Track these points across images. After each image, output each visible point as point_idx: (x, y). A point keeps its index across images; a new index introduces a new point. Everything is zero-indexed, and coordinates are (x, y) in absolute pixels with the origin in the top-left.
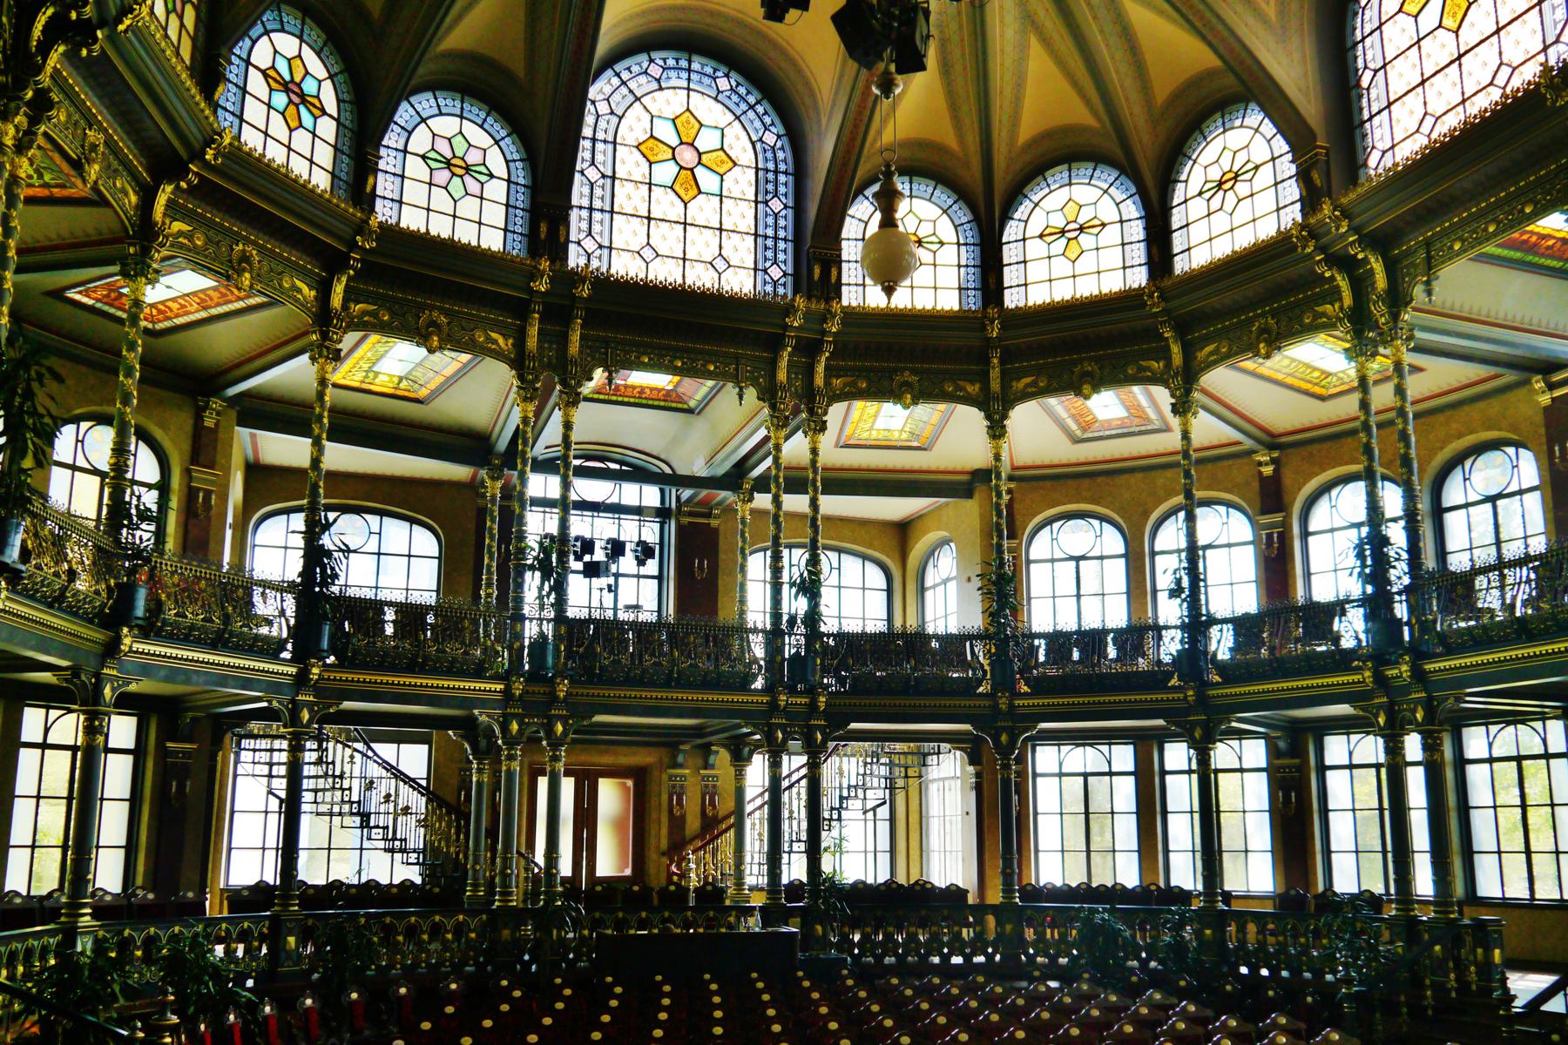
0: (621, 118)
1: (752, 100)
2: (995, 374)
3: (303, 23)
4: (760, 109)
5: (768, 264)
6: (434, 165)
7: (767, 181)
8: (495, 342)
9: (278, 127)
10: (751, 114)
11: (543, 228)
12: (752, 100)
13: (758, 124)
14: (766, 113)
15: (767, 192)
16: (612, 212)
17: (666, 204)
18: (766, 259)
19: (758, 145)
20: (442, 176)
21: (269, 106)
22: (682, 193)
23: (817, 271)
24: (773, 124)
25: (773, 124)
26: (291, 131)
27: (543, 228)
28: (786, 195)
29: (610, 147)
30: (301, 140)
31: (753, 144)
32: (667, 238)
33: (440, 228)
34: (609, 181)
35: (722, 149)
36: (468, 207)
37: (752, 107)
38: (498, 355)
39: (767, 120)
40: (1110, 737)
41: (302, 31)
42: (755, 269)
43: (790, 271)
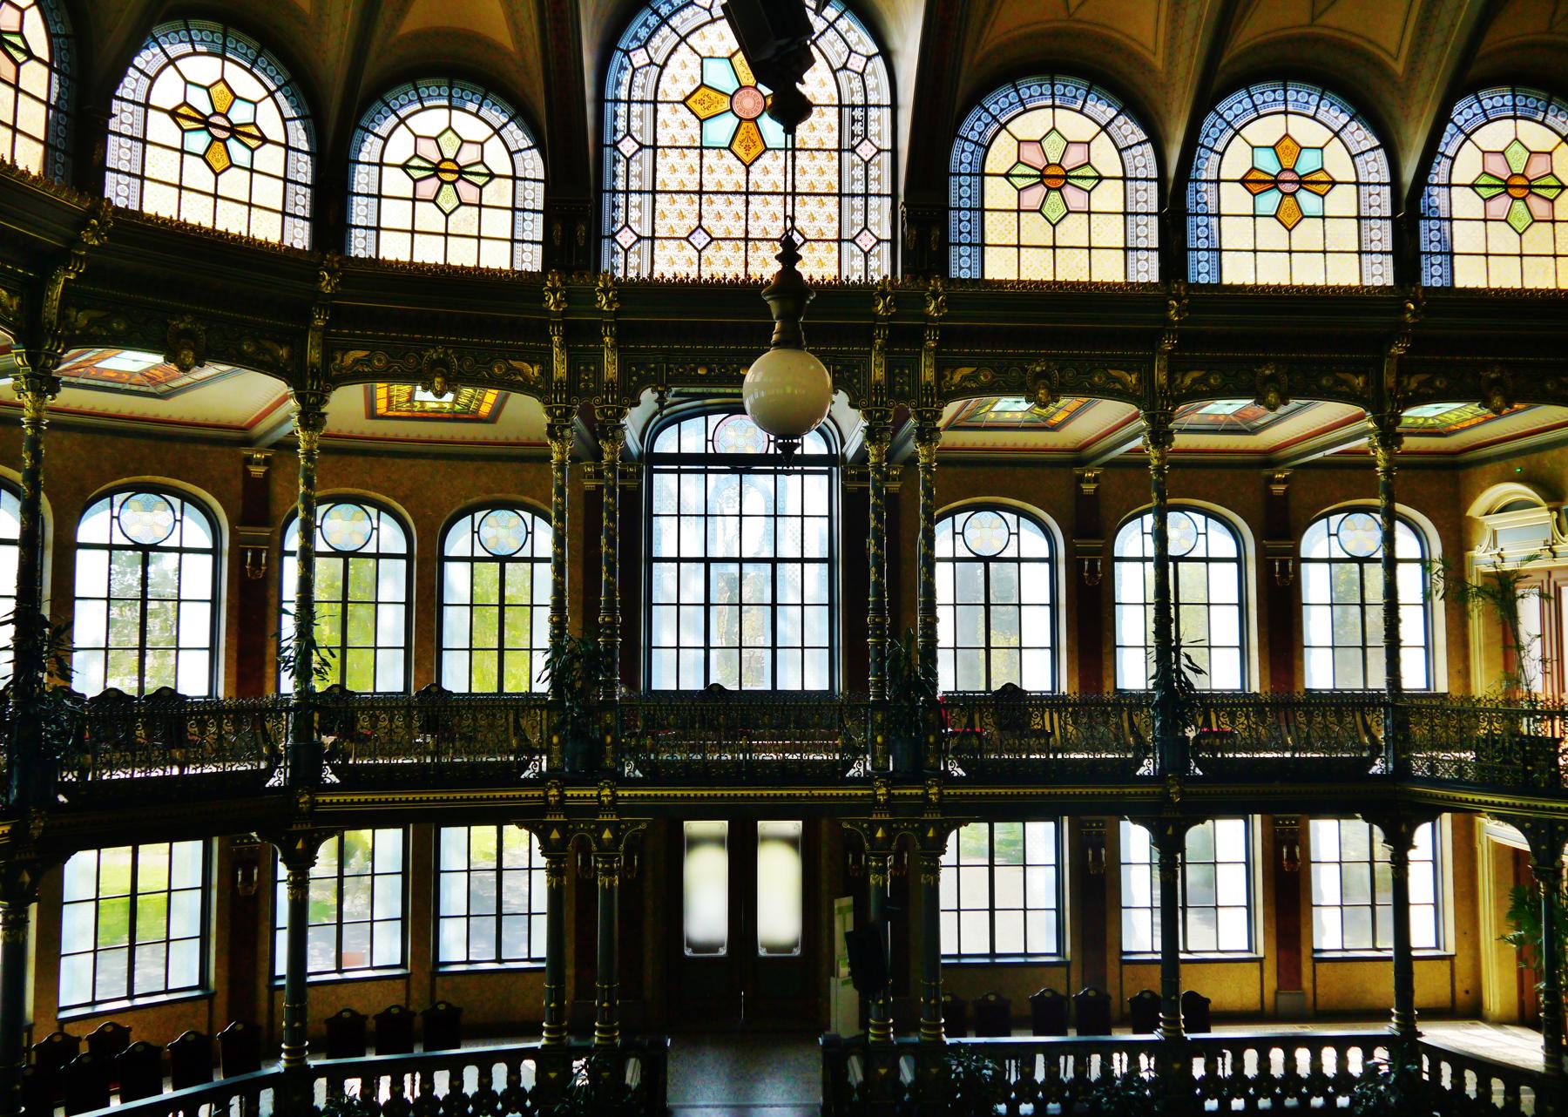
0: (662, 67)
3: (225, 36)
6: (417, 174)
7: (854, 121)
9: (196, 173)
17: (724, 171)
20: (428, 187)
21: (182, 152)
22: (741, 152)
26: (217, 175)
30: (233, 184)
31: (834, 72)
32: (724, 216)
33: (429, 253)
36: (464, 220)
38: (527, 388)
41: (224, 45)
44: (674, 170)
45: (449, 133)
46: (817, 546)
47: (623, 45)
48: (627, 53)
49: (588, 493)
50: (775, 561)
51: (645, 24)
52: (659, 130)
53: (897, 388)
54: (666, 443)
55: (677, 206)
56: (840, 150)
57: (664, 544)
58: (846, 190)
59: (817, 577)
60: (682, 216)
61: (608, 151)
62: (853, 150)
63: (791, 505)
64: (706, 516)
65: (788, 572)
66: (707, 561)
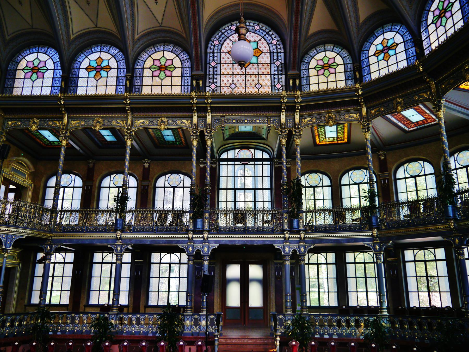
0: (222, 45)
1: (267, 31)
2: (364, 109)
4: (270, 33)
5: (276, 84)
7: (274, 56)
8: (184, 123)
10: (267, 36)
11: (194, 82)
12: (267, 31)
13: (270, 38)
14: (273, 34)
15: (274, 60)
16: (220, 75)
18: (275, 82)
19: (270, 45)
23: (291, 82)
24: (275, 37)
25: (275, 37)
27: (194, 82)
28: (281, 60)
29: (219, 54)
31: (268, 44)
32: (239, 80)
34: (219, 65)
35: (257, 48)
37: (267, 33)
39: (273, 36)
40: (435, 245)
42: (271, 86)
43: (284, 84)
44: (226, 69)
45: (165, 60)
46: (267, 184)
47: (212, 40)
48: (213, 41)
49: (201, 168)
50: (255, 189)
51: (218, 34)
52: (222, 60)
53: (288, 125)
54: (224, 156)
55: (227, 78)
56: (270, 63)
57: (223, 185)
58: (272, 73)
59: (267, 194)
60: (228, 81)
61: (208, 65)
62: (274, 63)
63: (259, 173)
64: (235, 177)
65: (259, 193)
66: (235, 189)
